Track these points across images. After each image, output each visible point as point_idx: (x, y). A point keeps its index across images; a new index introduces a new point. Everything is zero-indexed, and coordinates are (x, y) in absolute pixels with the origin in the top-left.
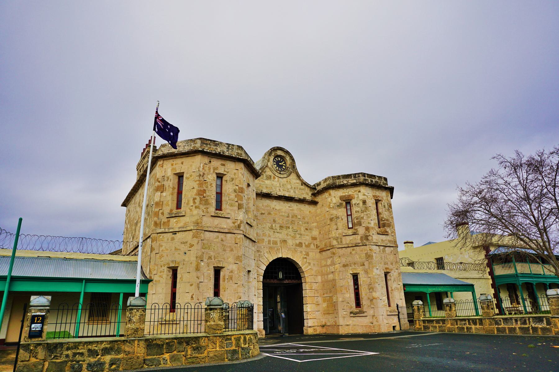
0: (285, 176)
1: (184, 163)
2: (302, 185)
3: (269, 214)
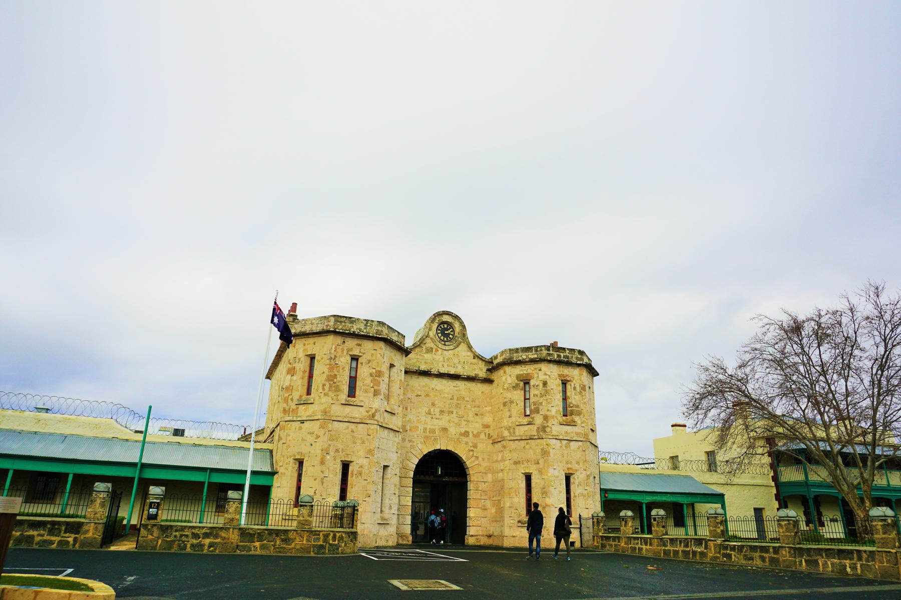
0: (452, 347)
1: (316, 343)
2: (474, 358)
3: (427, 395)
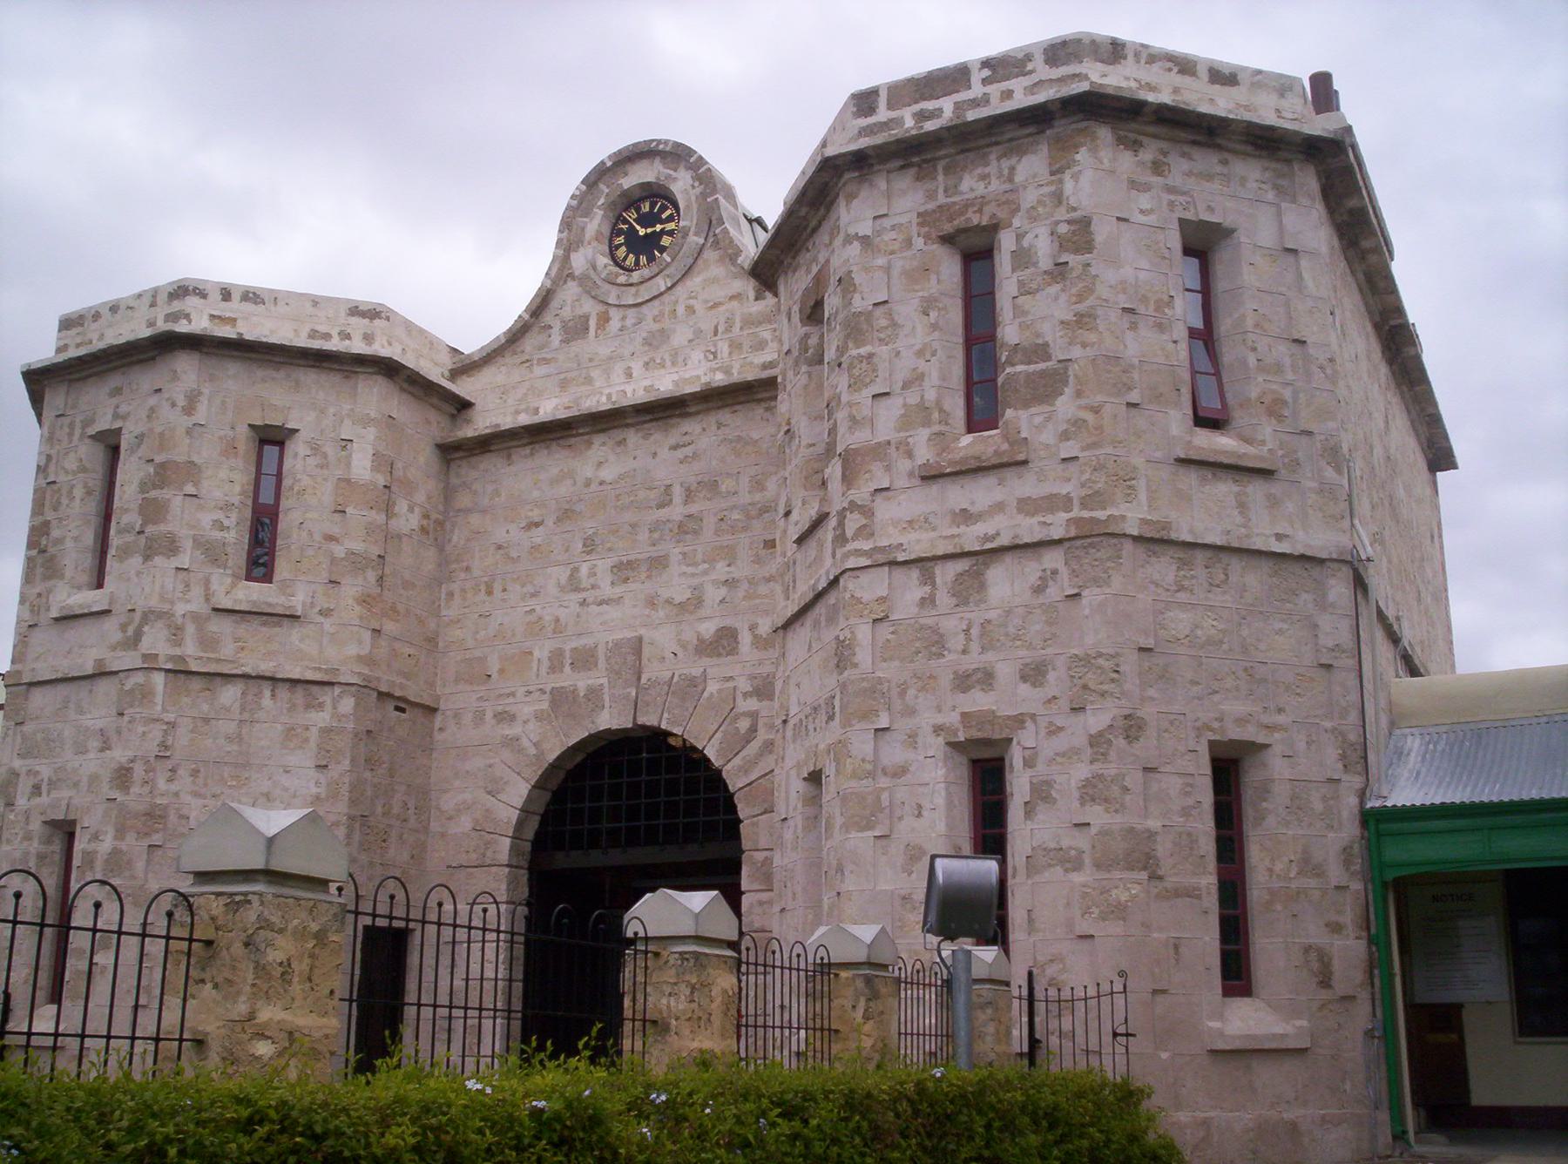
0: (661, 283)
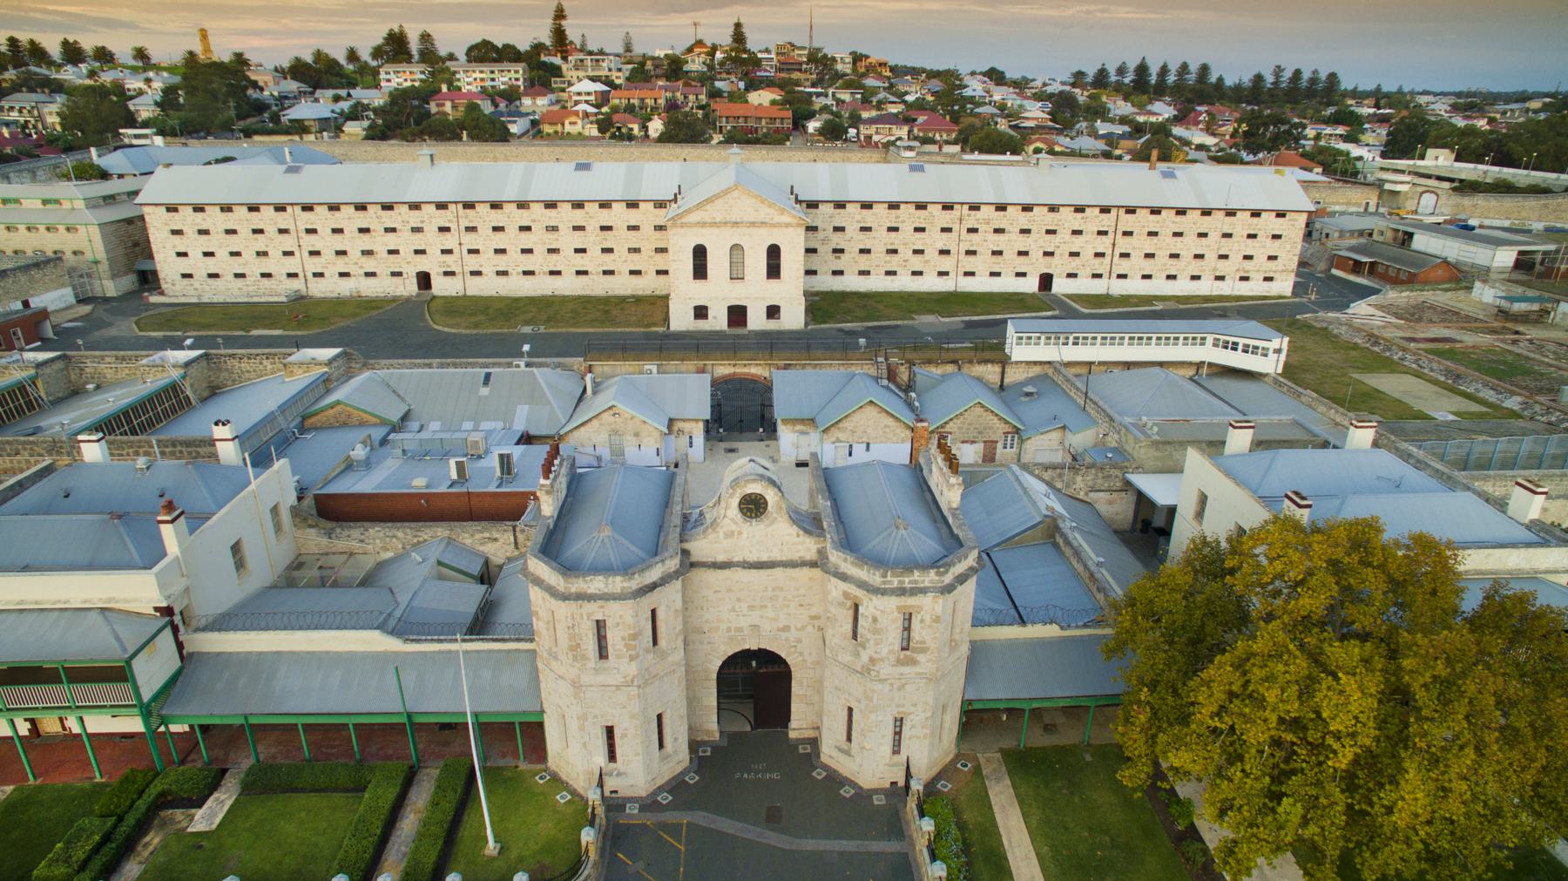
3: (729, 590)
